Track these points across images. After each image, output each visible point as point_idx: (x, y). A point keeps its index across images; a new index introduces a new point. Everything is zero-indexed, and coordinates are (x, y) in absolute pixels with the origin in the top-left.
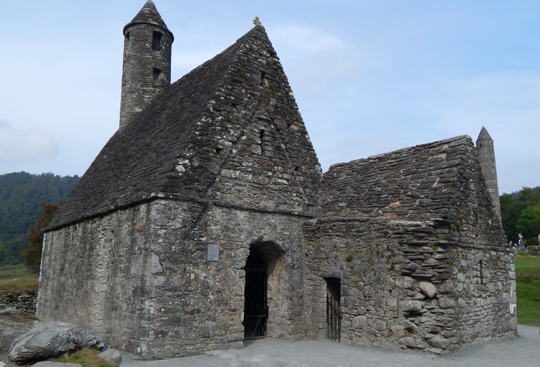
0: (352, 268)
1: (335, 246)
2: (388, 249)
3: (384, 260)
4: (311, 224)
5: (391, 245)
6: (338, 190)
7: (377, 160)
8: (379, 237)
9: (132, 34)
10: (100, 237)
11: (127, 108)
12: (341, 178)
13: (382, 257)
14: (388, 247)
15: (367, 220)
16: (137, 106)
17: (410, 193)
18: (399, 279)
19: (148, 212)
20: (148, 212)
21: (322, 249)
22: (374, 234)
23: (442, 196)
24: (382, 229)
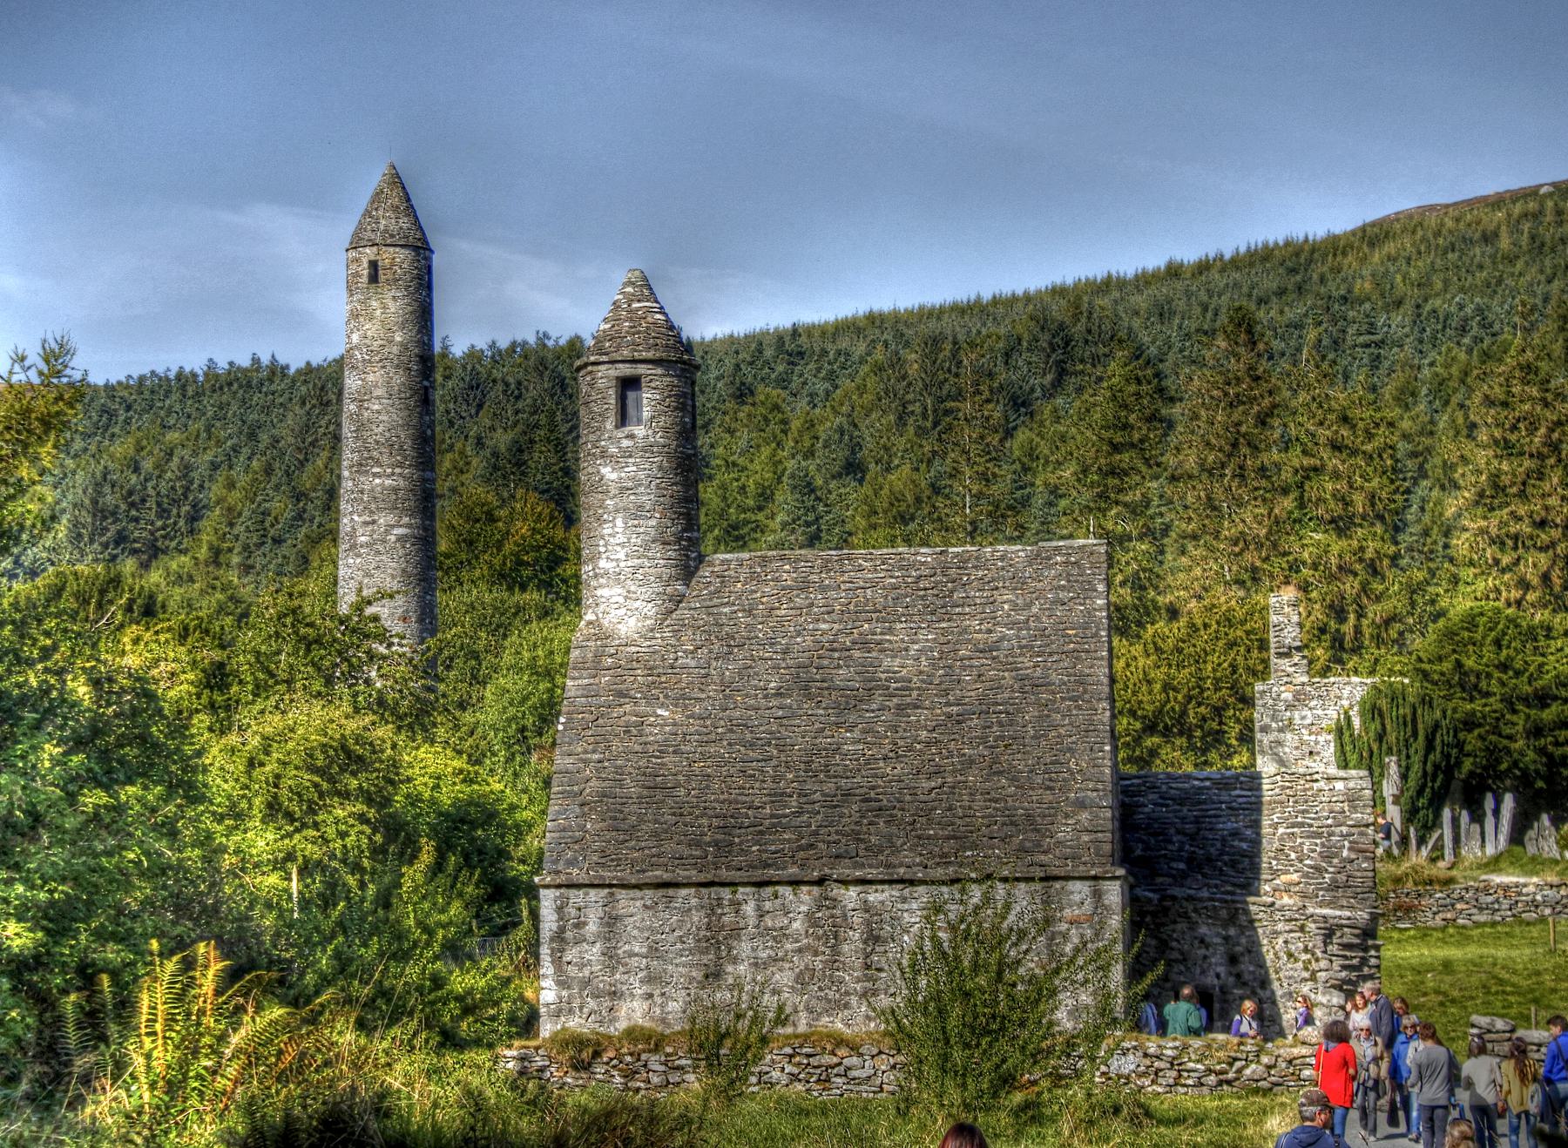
0: (1238, 976)
1: (1202, 941)
2: (1306, 950)
3: (1300, 965)
4: (1150, 900)
5: (1311, 945)
6: (1150, 834)
7: (1208, 783)
8: (1291, 931)
9: (652, 385)
10: (913, 920)
11: (652, 579)
12: (1146, 810)
13: (1296, 960)
14: (1306, 947)
15: (1273, 904)
16: (677, 580)
17: (1308, 862)
18: (1324, 994)
19: (1097, 895)
20: (1097, 895)
21: (1174, 944)
22: (1280, 926)
23: (1365, 874)
24: (1296, 920)
